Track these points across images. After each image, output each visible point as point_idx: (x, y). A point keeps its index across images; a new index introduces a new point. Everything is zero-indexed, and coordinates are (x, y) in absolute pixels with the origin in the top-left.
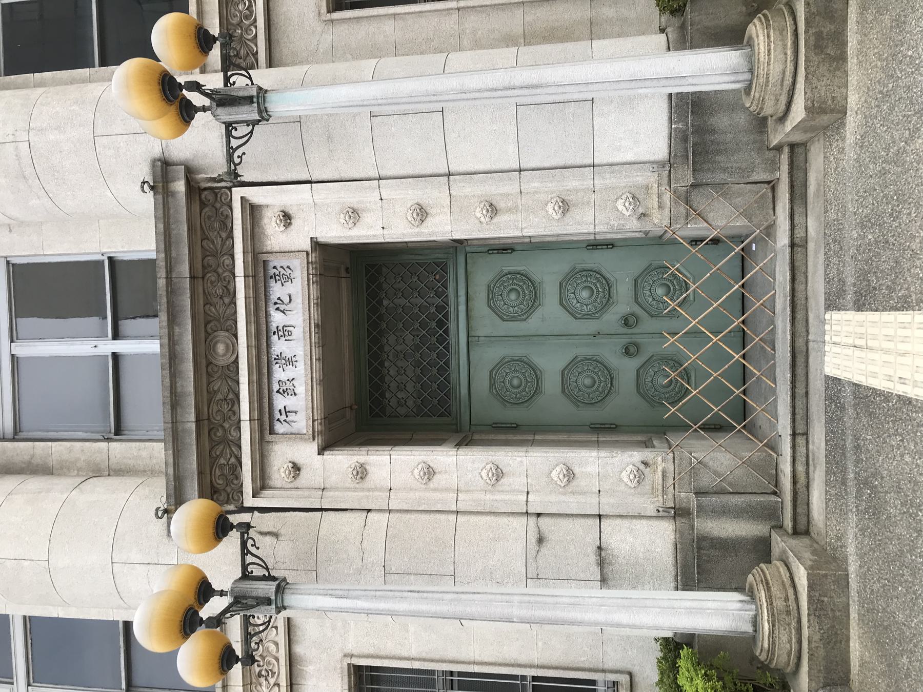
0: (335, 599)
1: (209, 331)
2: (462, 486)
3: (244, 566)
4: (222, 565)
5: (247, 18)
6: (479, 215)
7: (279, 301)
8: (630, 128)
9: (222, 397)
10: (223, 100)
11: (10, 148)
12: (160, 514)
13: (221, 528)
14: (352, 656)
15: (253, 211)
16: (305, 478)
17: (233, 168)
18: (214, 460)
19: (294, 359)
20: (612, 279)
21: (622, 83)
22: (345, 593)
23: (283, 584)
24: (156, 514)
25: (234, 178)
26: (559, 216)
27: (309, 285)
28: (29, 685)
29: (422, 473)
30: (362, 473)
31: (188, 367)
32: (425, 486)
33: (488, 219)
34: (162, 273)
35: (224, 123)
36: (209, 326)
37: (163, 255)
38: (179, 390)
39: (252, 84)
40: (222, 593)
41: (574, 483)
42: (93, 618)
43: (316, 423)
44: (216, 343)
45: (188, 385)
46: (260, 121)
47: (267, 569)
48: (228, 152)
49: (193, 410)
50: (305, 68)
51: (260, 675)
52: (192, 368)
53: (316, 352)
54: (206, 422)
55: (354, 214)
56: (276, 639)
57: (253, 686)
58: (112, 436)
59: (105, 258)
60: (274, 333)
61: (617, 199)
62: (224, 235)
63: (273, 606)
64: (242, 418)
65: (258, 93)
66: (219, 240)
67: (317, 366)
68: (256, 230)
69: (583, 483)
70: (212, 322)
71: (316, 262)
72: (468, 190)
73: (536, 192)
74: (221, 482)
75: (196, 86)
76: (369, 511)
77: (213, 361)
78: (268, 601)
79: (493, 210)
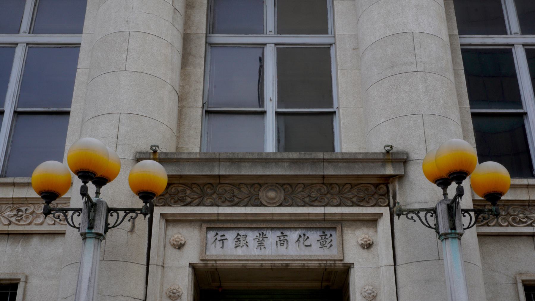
0: (88, 277)
1: (285, 186)
3: (116, 210)
4: (117, 193)
5: (514, 219)
7: (306, 237)
9: (235, 194)
10: (452, 209)
12: (154, 148)
13: (146, 195)
14: (26, 282)
15: (373, 221)
16: (172, 252)
17: (405, 213)
18: (190, 186)
19: (262, 247)
23: (102, 238)
24: (154, 146)
25: (396, 212)
27: (318, 260)
28: (27, 44)
30: (174, 297)
31: (259, 171)
34: (327, 156)
35: (436, 208)
36: (288, 186)
37: (340, 157)
38: (243, 164)
39: (464, 229)
40: (98, 193)
42: (74, 92)
43: (214, 262)
44: (276, 191)
45: (246, 171)
46: (439, 233)
47: (113, 227)
48: (416, 210)
49: (227, 174)
50: (479, 264)
51: (19, 210)
52: (259, 173)
53: (268, 264)
54: (218, 181)
56: (45, 224)
57: (11, 206)
58: (205, 108)
60: (282, 233)
62: (354, 200)
63: (87, 231)
64: (220, 208)
65: (458, 234)
66: (351, 196)
67: (257, 264)
70: (291, 189)
71: (335, 266)
74: (173, 190)
75: (460, 193)
77: (262, 189)
78: (91, 227)
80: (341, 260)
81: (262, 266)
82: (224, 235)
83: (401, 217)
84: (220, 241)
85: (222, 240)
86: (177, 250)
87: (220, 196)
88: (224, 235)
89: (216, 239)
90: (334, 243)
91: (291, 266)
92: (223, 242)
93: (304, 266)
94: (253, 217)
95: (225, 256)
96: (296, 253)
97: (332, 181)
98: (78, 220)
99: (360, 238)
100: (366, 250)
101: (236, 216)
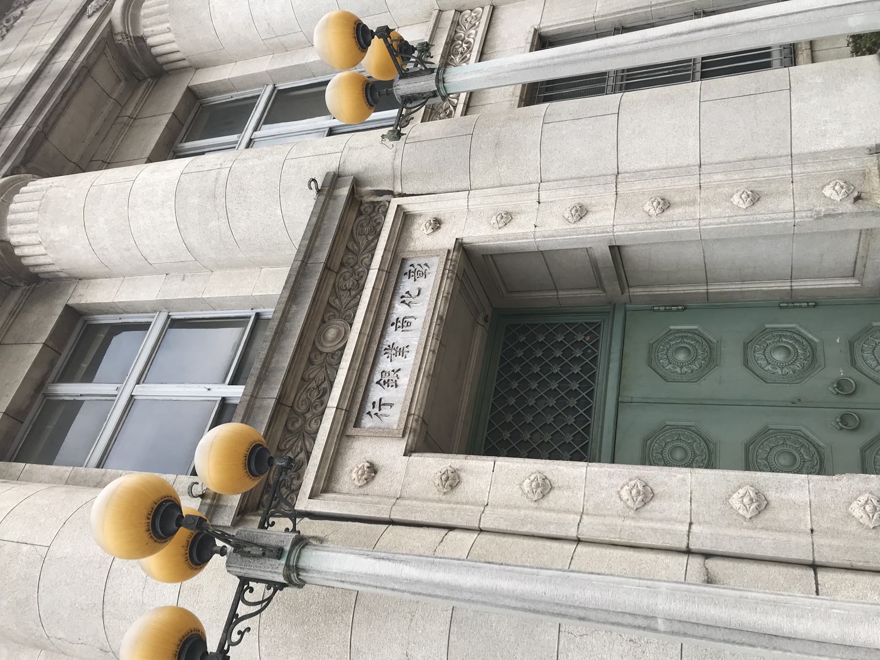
0: (373, 561)
1: (326, 319)
2: (590, 507)
6: (647, 207)
8: (838, 109)
11: (214, 173)
15: (405, 218)
19: (406, 349)
20: (816, 340)
21: (828, 10)
22: (390, 556)
24: (191, 487)
26: (747, 204)
29: (534, 484)
31: (291, 344)
32: (536, 505)
33: (658, 211)
37: (307, 242)
38: (272, 365)
41: (768, 515)
43: (411, 418)
45: (284, 361)
54: (288, 409)
55: (507, 217)
59: (253, 314)
60: (392, 324)
61: (823, 187)
62: (370, 238)
63: (283, 561)
64: (329, 404)
67: (429, 357)
68: (405, 234)
69: (783, 516)
71: (455, 261)
72: (638, 186)
76: (451, 528)
77: (320, 348)
78: (278, 552)
79: (666, 205)
80: (449, 251)
81: (434, 351)
82: (374, 403)
83: (403, 131)
86: (379, 477)
89: (376, 414)
90: (422, 261)
91: (443, 313)
92: (384, 404)
93: (447, 298)
94: (357, 359)
95: (405, 399)
96: (426, 307)
97: (338, 263)
100: (442, 226)
101: (350, 383)
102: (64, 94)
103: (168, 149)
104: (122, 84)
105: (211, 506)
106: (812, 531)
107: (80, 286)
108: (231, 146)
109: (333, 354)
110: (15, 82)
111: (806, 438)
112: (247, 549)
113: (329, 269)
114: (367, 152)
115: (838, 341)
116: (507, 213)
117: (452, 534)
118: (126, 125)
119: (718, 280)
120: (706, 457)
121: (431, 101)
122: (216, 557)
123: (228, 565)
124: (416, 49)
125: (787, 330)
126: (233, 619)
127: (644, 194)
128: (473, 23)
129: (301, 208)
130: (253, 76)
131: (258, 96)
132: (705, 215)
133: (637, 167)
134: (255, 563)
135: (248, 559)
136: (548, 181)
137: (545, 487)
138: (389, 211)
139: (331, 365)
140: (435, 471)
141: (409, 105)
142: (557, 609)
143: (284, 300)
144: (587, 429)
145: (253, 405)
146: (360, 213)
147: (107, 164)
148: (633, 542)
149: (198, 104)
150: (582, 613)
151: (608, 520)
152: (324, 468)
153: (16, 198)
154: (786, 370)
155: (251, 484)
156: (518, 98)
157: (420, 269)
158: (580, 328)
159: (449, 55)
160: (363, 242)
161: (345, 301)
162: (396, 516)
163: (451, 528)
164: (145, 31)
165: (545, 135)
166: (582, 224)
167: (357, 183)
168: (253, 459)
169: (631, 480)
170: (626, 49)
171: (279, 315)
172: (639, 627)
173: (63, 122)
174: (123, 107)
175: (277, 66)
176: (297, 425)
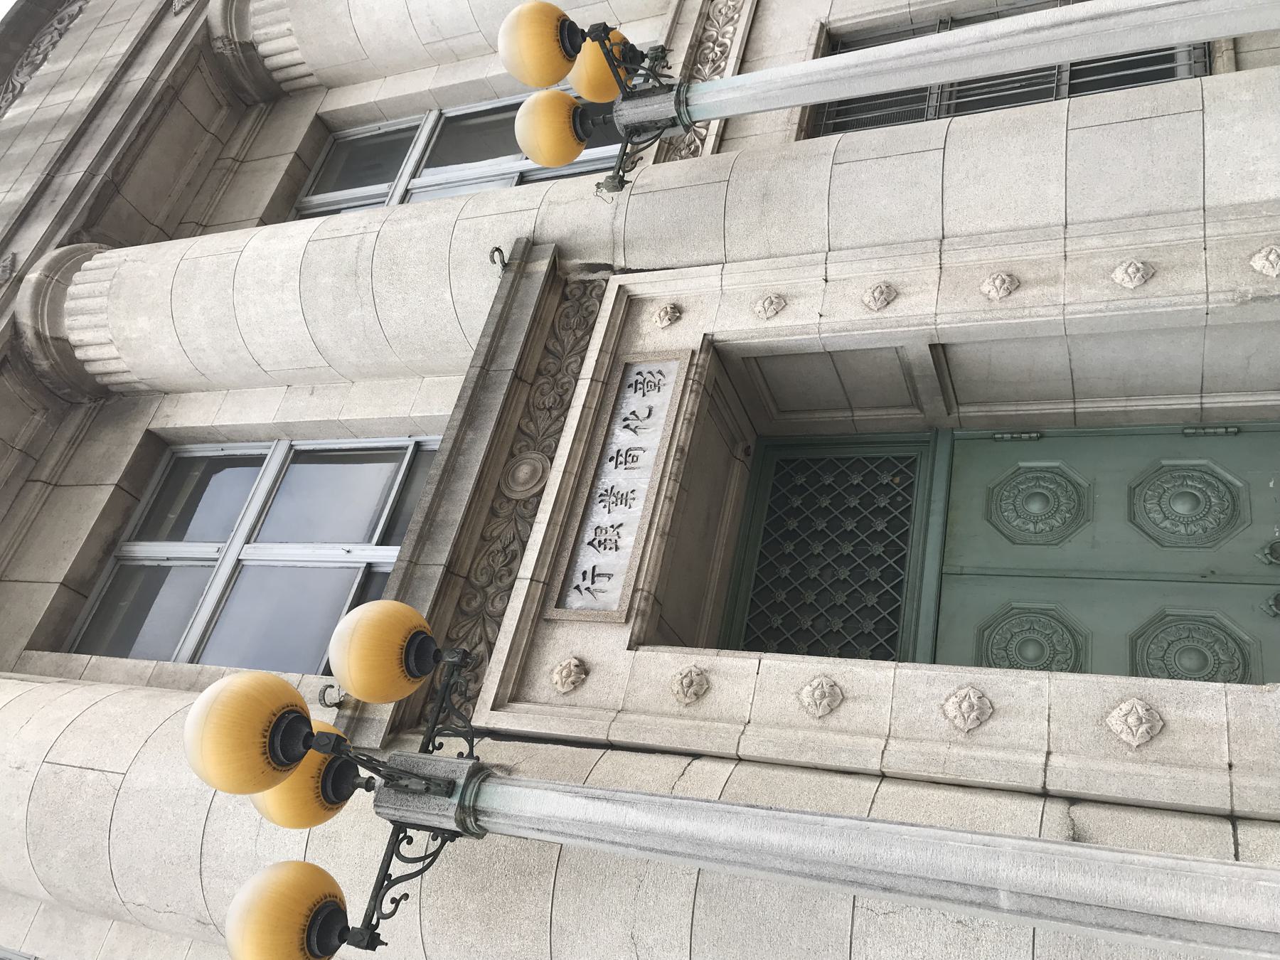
0: (584, 801)
1: (516, 452)
2: (899, 727)
6: (986, 288)
15: (630, 305)
16: (592, 690)
19: (631, 496)
20: (1238, 483)
22: (608, 794)
24: (323, 692)
26: (1136, 282)
29: (817, 693)
31: (466, 487)
32: (820, 723)
38: (440, 517)
41: (1164, 742)
43: (639, 594)
45: (456, 512)
54: (462, 581)
55: (779, 303)
61: (1251, 257)
62: (579, 333)
63: (455, 800)
67: (665, 507)
68: (629, 328)
69: (1188, 744)
71: (703, 366)
72: (973, 256)
73: (1093, 256)
76: (696, 756)
77: (507, 493)
78: (449, 788)
79: (1014, 283)
80: (693, 353)
81: (671, 499)
82: (585, 573)
83: (628, 177)
84: (593, 583)
85: (593, 576)
86: (592, 680)
87: (494, 577)
88: (585, 573)
89: (587, 589)
90: (654, 368)
91: (685, 443)
92: (599, 575)
93: (690, 421)
94: (560, 510)
95: (630, 568)
96: (659, 434)
97: (533, 370)
98: (421, 842)
99: (658, 324)
101: (550, 544)
102: (142, 127)
103: (289, 206)
104: (224, 112)
105: (351, 719)
106: (1230, 766)
107: (166, 403)
108: (378, 201)
109: (526, 502)
110: (72, 110)
111: (1222, 628)
112: (404, 782)
113: (520, 379)
114: (575, 208)
115: (1271, 485)
116: (779, 296)
117: (697, 763)
118: (229, 170)
119: (1090, 395)
120: (1075, 659)
121: (669, 133)
122: (360, 792)
123: (377, 803)
124: (646, 56)
125: (1194, 468)
126: (384, 881)
127: (981, 267)
128: (730, 15)
129: (480, 290)
130: (409, 98)
131: (417, 127)
132: (1072, 300)
133: (972, 228)
134: (415, 802)
135: (405, 796)
136: (840, 249)
137: (834, 698)
138: (607, 294)
139: (523, 518)
140: (674, 672)
141: (636, 139)
142: (851, 875)
143: (456, 423)
144: (896, 614)
145: (411, 576)
146: (564, 298)
147: (203, 228)
148: (962, 779)
149: (331, 139)
150: (887, 881)
151: (927, 747)
152: (513, 666)
153: (77, 277)
154: (1192, 528)
155: (409, 688)
156: (795, 127)
157: (652, 379)
158: (886, 464)
159: (694, 64)
160: (569, 340)
161: (543, 425)
162: (616, 737)
163: (696, 756)
164: (255, 34)
165: (836, 182)
166: (888, 313)
167: (560, 254)
168: (413, 653)
169: (960, 688)
170: (957, 53)
171: (449, 445)
172: (972, 903)
173: (142, 169)
174: (225, 145)
175: (445, 82)
176: (475, 604)
